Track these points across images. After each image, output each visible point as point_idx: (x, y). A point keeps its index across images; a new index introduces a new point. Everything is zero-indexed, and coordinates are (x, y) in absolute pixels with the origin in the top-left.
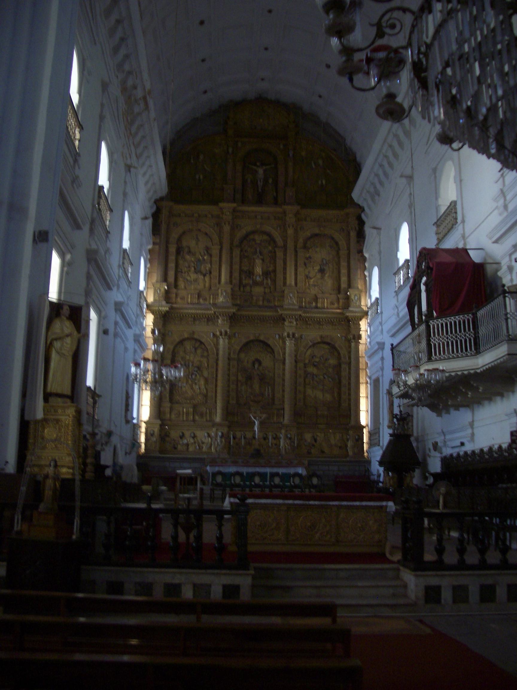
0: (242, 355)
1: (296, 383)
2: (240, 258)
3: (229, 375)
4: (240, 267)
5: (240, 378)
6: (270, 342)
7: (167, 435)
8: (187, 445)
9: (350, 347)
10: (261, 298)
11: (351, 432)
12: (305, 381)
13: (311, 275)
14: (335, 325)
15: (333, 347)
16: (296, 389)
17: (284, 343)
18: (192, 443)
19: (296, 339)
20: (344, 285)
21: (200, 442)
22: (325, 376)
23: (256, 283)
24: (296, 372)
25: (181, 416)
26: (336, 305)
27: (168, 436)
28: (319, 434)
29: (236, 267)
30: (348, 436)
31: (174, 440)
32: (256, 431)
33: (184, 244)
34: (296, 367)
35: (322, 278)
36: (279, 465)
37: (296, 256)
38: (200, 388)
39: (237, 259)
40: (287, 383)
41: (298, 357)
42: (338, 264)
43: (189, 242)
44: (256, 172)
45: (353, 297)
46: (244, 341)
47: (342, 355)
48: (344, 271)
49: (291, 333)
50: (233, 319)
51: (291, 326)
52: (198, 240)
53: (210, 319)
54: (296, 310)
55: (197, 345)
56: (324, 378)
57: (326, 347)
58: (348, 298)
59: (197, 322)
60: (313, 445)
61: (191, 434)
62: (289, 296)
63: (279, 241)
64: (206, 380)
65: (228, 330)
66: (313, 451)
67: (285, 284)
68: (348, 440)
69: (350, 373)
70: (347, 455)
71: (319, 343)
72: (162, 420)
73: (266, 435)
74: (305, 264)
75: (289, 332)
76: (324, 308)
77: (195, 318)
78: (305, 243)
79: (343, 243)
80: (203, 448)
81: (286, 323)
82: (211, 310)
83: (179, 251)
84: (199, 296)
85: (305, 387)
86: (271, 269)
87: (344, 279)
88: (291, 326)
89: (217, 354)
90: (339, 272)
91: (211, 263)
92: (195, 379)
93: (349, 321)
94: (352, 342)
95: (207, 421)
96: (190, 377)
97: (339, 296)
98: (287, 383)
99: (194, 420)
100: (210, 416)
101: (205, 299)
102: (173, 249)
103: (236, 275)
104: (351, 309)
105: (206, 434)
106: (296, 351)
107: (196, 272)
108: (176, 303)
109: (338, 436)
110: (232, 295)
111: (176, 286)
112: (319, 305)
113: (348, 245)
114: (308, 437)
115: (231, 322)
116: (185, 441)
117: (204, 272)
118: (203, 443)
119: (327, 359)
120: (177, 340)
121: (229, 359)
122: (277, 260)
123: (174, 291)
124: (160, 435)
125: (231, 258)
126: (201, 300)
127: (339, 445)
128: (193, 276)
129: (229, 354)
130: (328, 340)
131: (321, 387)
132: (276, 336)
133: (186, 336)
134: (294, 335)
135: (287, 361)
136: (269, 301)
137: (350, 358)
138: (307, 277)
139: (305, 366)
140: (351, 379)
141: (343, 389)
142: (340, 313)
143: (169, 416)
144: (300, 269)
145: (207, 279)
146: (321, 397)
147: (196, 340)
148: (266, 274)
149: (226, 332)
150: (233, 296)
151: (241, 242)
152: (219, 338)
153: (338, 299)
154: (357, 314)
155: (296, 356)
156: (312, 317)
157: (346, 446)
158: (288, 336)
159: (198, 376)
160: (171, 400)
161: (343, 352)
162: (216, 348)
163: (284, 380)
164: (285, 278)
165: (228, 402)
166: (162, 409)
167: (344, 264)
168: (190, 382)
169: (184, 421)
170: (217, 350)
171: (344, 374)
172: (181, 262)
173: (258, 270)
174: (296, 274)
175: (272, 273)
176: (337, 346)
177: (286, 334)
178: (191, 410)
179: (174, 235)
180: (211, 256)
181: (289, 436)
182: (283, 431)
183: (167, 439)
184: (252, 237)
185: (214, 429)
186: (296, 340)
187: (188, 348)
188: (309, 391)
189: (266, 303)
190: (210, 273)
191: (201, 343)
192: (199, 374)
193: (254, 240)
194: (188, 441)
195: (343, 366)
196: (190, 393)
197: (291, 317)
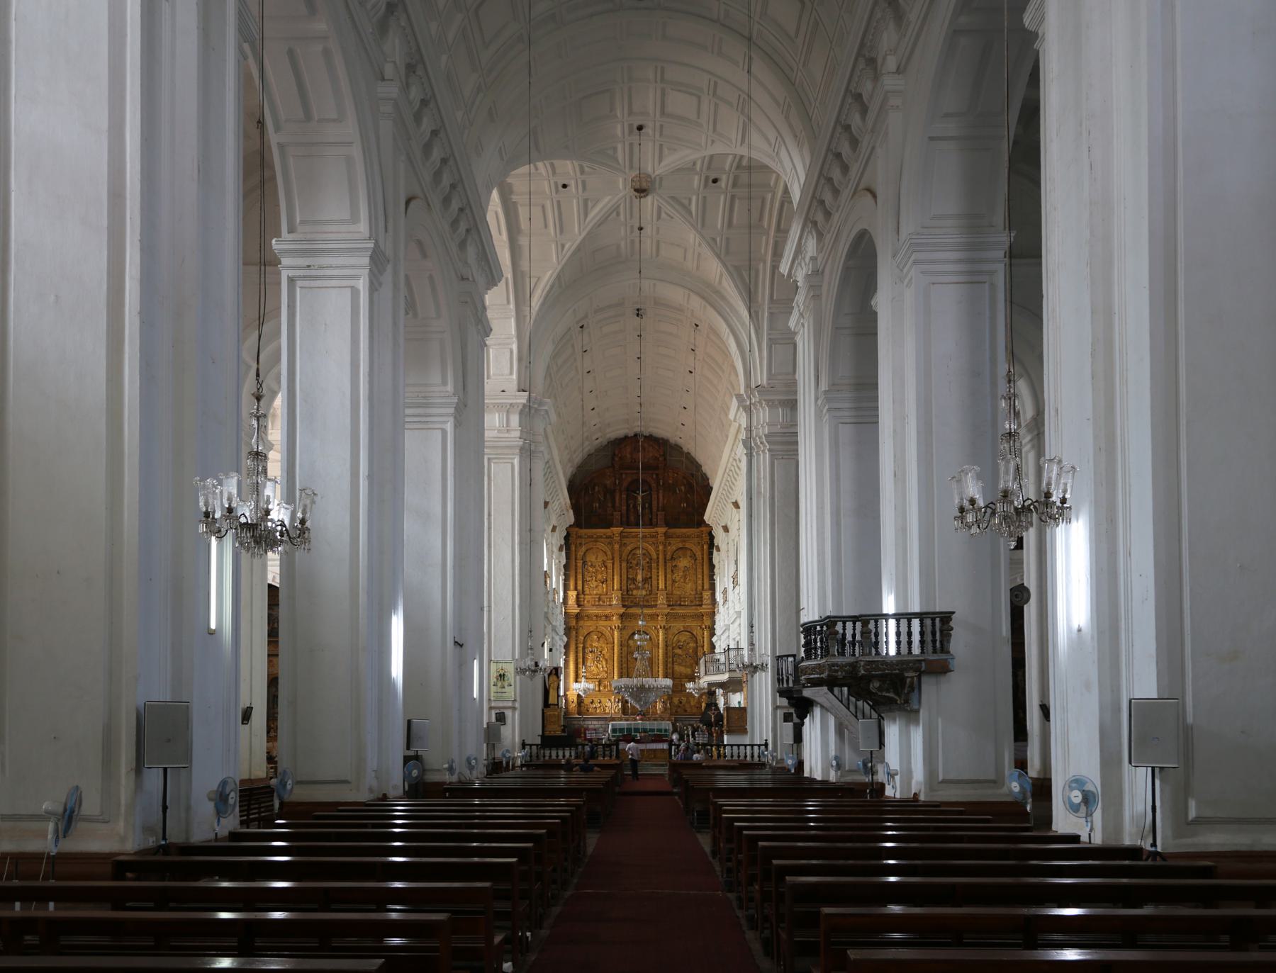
0: (631, 642)
1: (667, 661)
2: (627, 569)
4: (627, 575)
9: (703, 634)
12: (673, 660)
13: (677, 579)
15: (693, 634)
16: (667, 665)
17: (658, 632)
23: (637, 588)
24: (667, 654)
29: (624, 577)
33: (588, 559)
34: (666, 650)
37: (665, 566)
39: (624, 571)
40: (661, 662)
42: (696, 570)
43: (591, 558)
48: (700, 576)
50: (622, 616)
54: (665, 609)
57: (688, 634)
60: (679, 707)
63: (655, 556)
66: (679, 710)
67: (658, 587)
74: (672, 571)
79: (698, 554)
81: (659, 618)
83: (584, 563)
84: (600, 599)
85: (673, 664)
86: (648, 576)
87: (700, 582)
91: (607, 573)
93: (703, 615)
98: (661, 662)
101: (604, 602)
102: (580, 564)
103: (624, 582)
104: (703, 606)
107: (596, 581)
110: (622, 598)
111: (583, 592)
112: (682, 603)
113: (703, 554)
114: (676, 701)
115: (622, 619)
117: (602, 580)
123: (582, 596)
125: (621, 569)
126: (601, 603)
130: (689, 630)
131: (684, 664)
134: (664, 627)
135: (660, 646)
137: (703, 642)
138: (674, 581)
139: (673, 649)
144: (669, 576)
145: (604, 586)
148: (645, 580)
149: (618, 626)
150: (623, 599)
153: (695, 598)
155: (666, 642)
158: (661, 627)
161: (699, 638)
163: (658, 660)
164: (658, 584)
167: (699, 570)
172: (586, 573)
173: (639, 578)
174: (666, 580)
176: (695, 633)
177: (659, 627)
179: (580, 554)
180: (606, 567)
184: (633, 552)
188: (677, 668)
189: (645, 603)
195: (699, 648)
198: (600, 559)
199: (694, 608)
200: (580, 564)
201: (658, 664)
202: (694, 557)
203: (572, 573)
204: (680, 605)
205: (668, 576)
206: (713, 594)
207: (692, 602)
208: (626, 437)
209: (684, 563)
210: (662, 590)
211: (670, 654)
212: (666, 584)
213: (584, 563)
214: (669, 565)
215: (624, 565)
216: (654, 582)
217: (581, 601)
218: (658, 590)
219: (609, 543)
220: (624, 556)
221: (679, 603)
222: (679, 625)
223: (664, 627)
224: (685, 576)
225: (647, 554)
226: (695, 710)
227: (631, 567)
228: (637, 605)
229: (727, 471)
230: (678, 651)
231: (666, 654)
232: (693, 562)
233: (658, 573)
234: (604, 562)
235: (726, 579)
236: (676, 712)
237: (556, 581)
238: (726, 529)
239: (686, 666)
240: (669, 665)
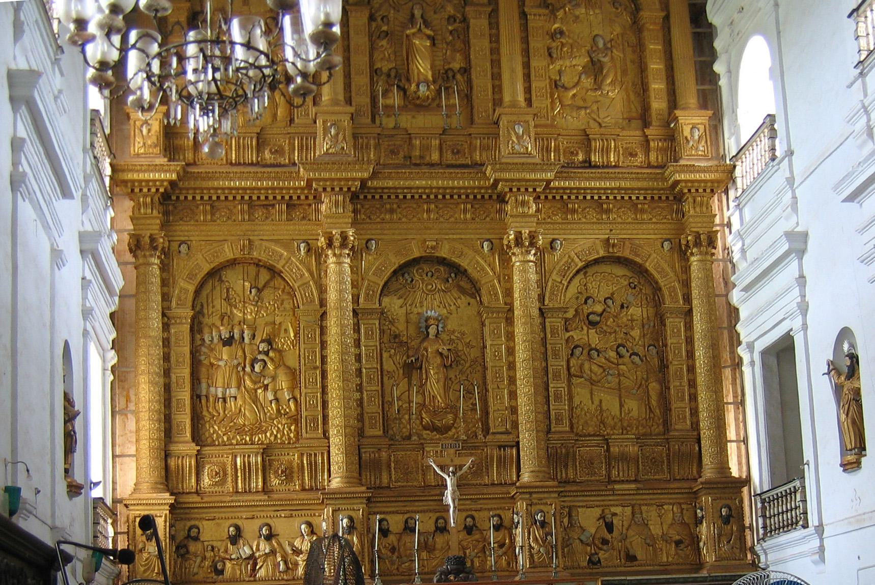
0: (393, 304)
3: (358, 358)
5: (389, 365)
6: (464, 263)
8: (252, 557)
9: (686, 269)
10: (435, 142)
11: (706, 500)
12: (568, 369)
14: (642, 211)
15: (640, 271)
17: (506, 262)
18: (266, 555)
19: (538, 249)
20: (658, 104)
21: (288, 550)
22: (622, 350)
23: (414, 104)
24: (544, 341)
25: (229, 479)
26: (641, 158)
27: (196, 539)
28: (618, 510)
30: (699, 511)
31: (213, 548)
32: (448, 505)
35: (598, 86)
38: (277, 400)
41: (546, 302)
45: (687, 132)
46: (396, 262)
47: (666, 292)
49: (525, 232)
51: (524, 215)
54: (534, 168)
55: (264, 276)
56: (620, 356)
57: (619, 271)
58: (671, 138)
59: (259, 213)
60: (605, 542)
61: (261, 529)
62: (516, 133)
64: (294, 375)
65: (351, 232)
66: (601, 554)
67: (498, 102)
68: (698, 522)
69: (690, 341)
70: (700, 566)
71: (597, 261)
72: (172, 494)
73: (473, 518)
75: (520, 233)
76: (608, 167)
80: (296, 564)
81: (508, 208)
82: (299, 178)
84: (261, 142)
86: (456, 66)
88: (524, 215)
89: (323, 303)
90: (642, 69)
92: (262, 374)
93: (679, 198)
94: (692, 254)
95: (304, 489)
96: (248, 369)
97: (647, 132)
98: (522, 373)
99: (266, 490)
100: (313, 475)
101: (279, 152)
103: (361, 81)
104: (682, 162)
105: (303, 526)
106: (542, 284)
108: (194, 164)
109: (670, 512)
110: (355, 136)
112: (595, 158)
115: (355, 211)
116: (247, 551)
118: (297, 552)
119: (625, 305)
120: (206, 268)
121: (355, 312)
122: (473, 41)
126: (267, 155)
127: (677, 538)
129: (356, 299)
130: (627, 254)
132: (483, 247)
133: (228, 253)
134: (532, 237)
136: (457, 152)
137: (688, 298)
140: (697, 354)
141: (674, 384)
143: (193, 480)
146: (615, 410)
147: (258, 264)
152: (327, 256)
154: (702, 176)
155: (541, 298)
156: (578, 189)
157: (695, 540)
158: (518, 241)
159: (270, 366)
160: (197, 437)
161: (668, 281)
162: (315, 283)
163: (512, 366)
164: (497, 89)
165: (361, 433)
166: (172, 463)
168: (248, 382)
169: (237, 492)
170: (322, 290)
171: (674, 339)
175: (458, 76)
176: (649, 266)
178: (256, 460)
181: (539, 517)
182: (521, 505)
183: (193, 547)
185: (328, 511)
186: (540, 252)
187: (239, 289)
188: (582, 395)
189: (449, 158)
191: (274, 272)
192: (272, 359)
194: (254, 549)
196: (248, 416)
197: (523, 190)
201: (512, 380)
204: (588, 164)
205: (534, 63)
210: (514, 104)
211: (558, 342)
214: (534, 22)
216: (481, 81)
221: (581, 157)
223: (532, 237)
226: (667, 554)
228: (420, 164)
230: (594, 338)
236: (593, 562)
240: (551, 385)
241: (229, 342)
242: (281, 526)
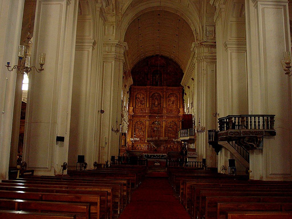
4: (152, 102)
7: (134, 145)
17: (163, 122)
29: (151, 103)
36: (161, 153)
44: (156, 76)
50: (150, 117)
52: (141, 95)
53: (144, 117)
54: (165, 114)
58: (179, 110)
63: (162, 95)
64: (143, 131)
67: (163, 108)
77: (141, 116)
78: (169, 95)
83: (136, 98)
93: (180, 117)
99: (140, 142)
102: (134, 98)
111: (135, 107)
112: (172, 112)
124: (132, 146)
128: (140, 105)
134: (165, 120)
136: (159, 111)
137: (180, 126)
142: (178, 115)
151: (152, 95)
158: (164, 120)
161: (178, 124)
170: (146, 124)
173: (156, 103)
174: (166, 104)
190: (144, 104)
193: (155, 95)
198: (142, 97)
199: (176, 114)
200: (134, 98)
202: (177, 97)
203: (132, 101)
204: (171, 113)
206: (184, 109)
207: (175, 112)
208: (153, 56)
209: (172, 99)
212: (166, 106)
213: (136, 98)
215: (151, 99)
216: (162, 105)
217: (134, 111)
218: (163, 108)
219: (146, 91)
220: (151, 96)
222: (170, 120)
224: (173, 103)
225: (159, 95)
227: (154, 100)
228: (155, 113)
229: (190, 68)
231: (165, 130)
232: (176, 98)
233: (163, 102)
234: (143, 98)
235: (188, 104)
236: (169, 150)
237: (126, 104)
238: (189, 87)
239: (173, 134)
241: (138, 128)
242: (141, 145)
